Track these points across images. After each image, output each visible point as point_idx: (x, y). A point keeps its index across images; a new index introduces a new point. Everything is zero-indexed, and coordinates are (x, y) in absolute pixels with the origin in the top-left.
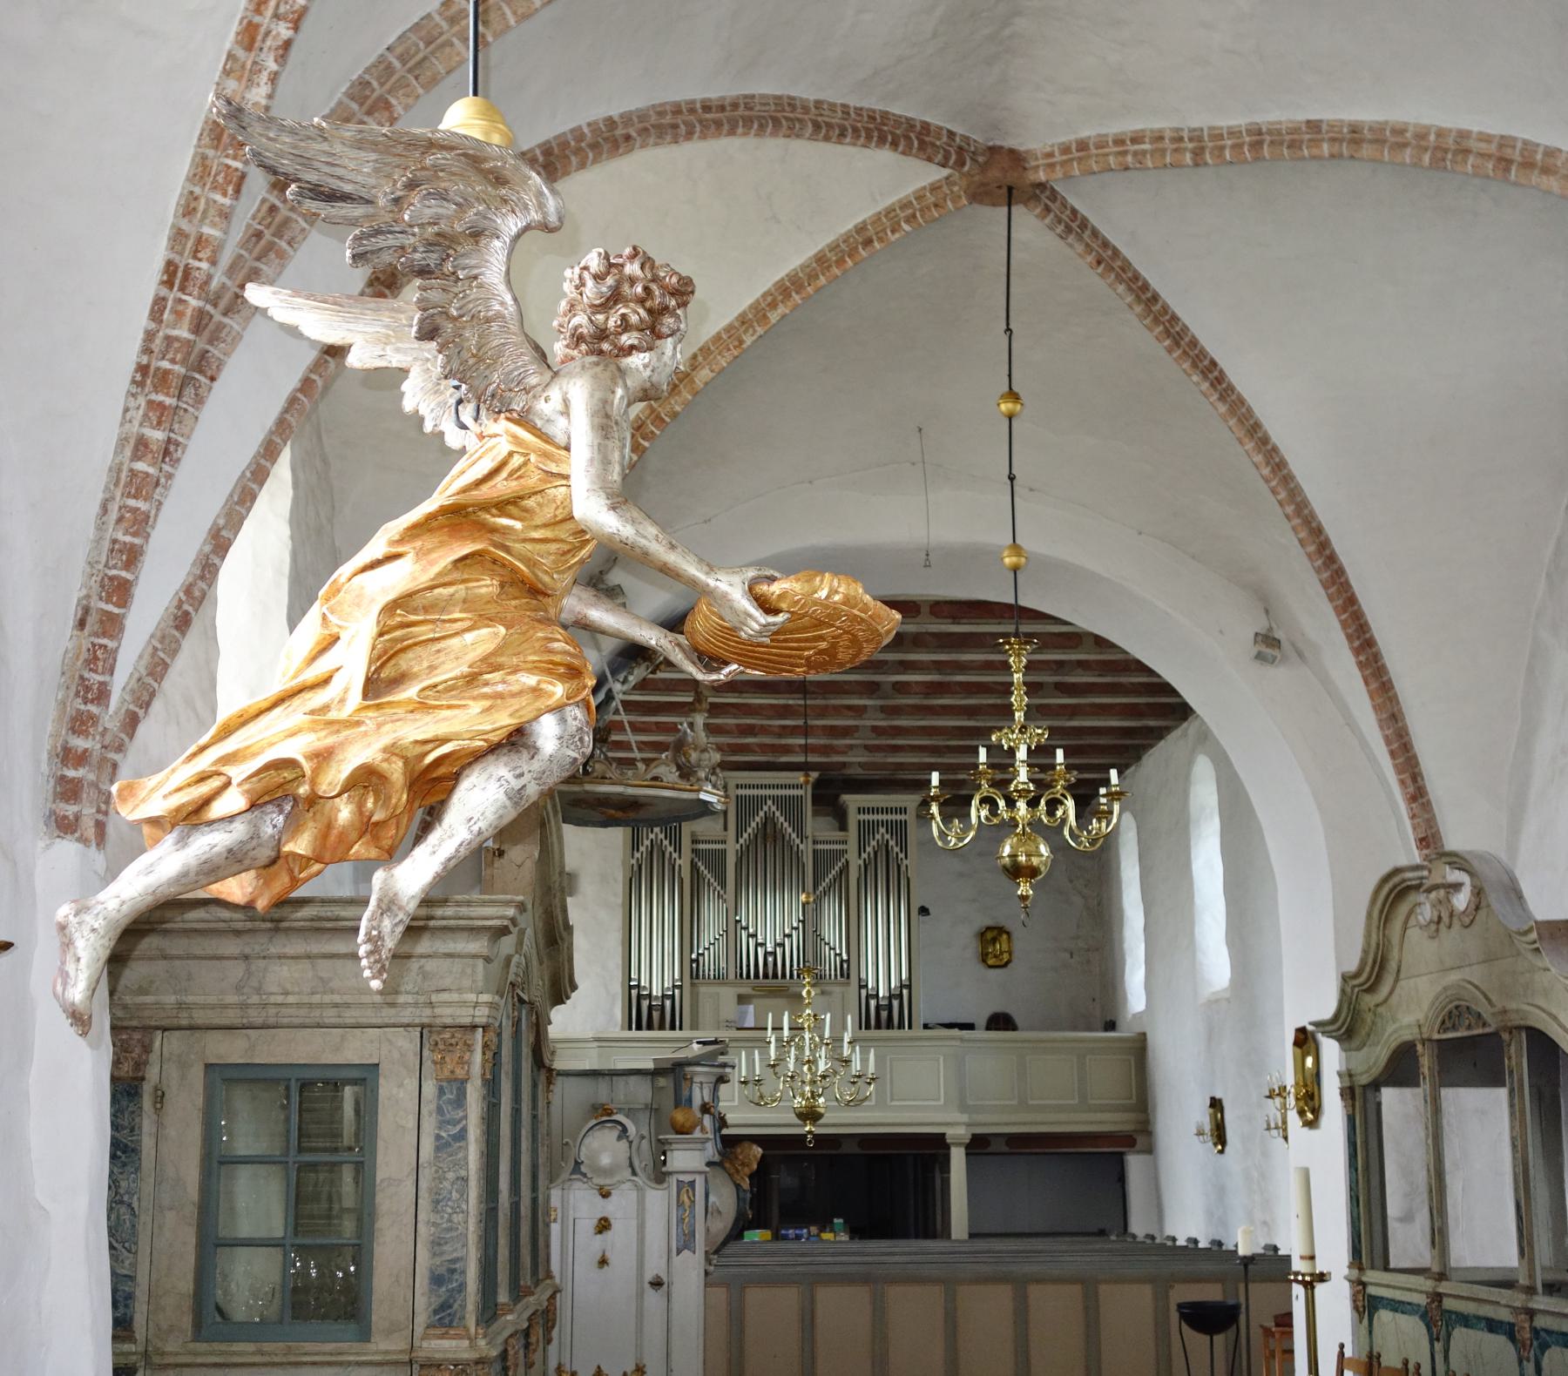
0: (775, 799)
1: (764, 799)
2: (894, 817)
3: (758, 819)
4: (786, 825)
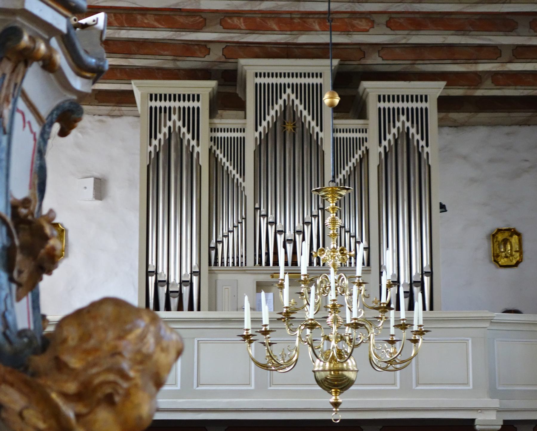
0: (295, 88)
1: (282, 88)
2: (415, 105)
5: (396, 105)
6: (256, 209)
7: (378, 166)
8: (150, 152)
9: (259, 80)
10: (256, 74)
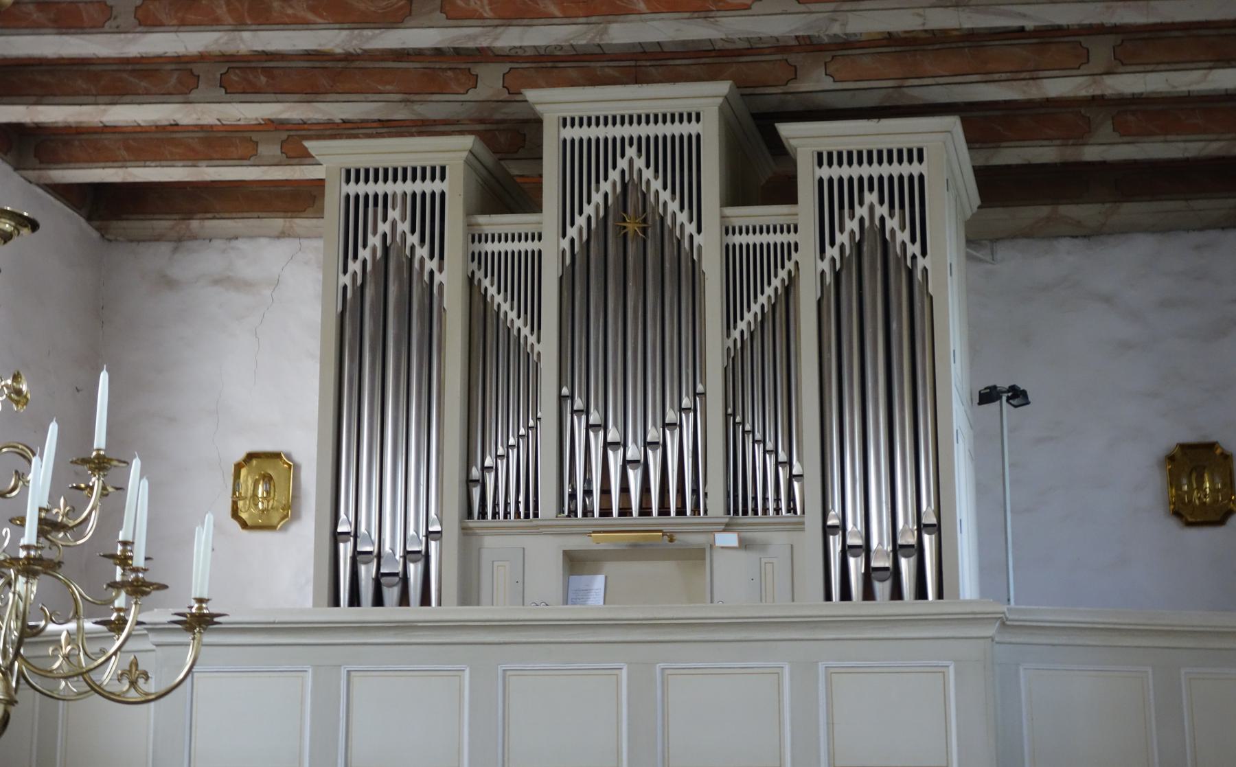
0: (642, 144)
1: (617, 147)
2: (895, 169)
3: (606, 186)
4: (665, 196)
5: (855, 171)
6: (561, 398)
7: (819, 302)
8: (345, 288)
9: (569, 133)
10: (565, 120)
